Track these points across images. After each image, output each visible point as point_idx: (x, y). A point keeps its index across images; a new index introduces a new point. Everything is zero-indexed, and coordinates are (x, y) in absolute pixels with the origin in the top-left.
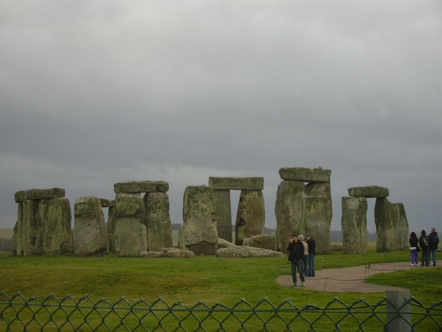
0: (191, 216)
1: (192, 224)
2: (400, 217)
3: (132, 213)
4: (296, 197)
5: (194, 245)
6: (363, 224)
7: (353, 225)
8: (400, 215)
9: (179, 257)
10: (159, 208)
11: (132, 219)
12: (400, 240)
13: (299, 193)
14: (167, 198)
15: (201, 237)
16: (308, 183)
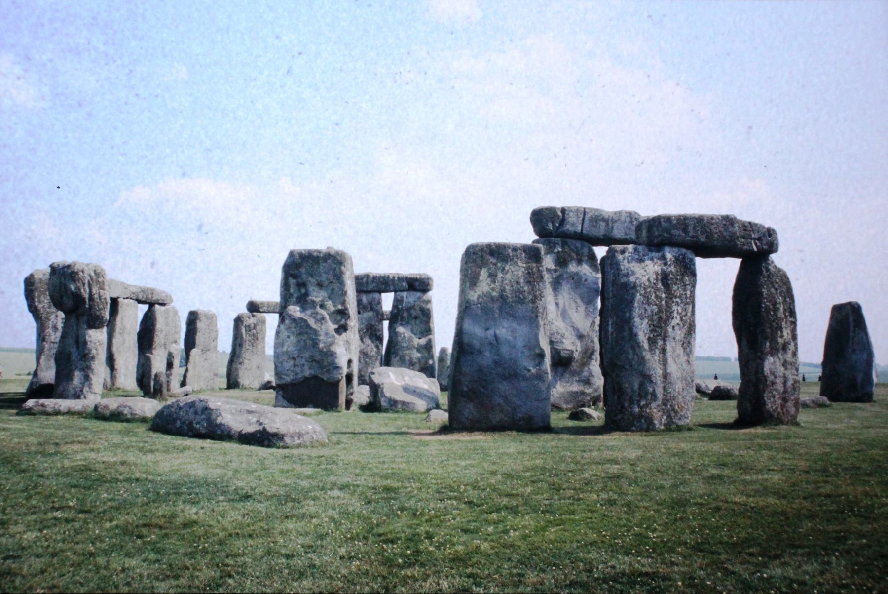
0: (287, 317)
6: (676, 332)
7: (633, 336)
10: (416, 318)
15: (306, 368)
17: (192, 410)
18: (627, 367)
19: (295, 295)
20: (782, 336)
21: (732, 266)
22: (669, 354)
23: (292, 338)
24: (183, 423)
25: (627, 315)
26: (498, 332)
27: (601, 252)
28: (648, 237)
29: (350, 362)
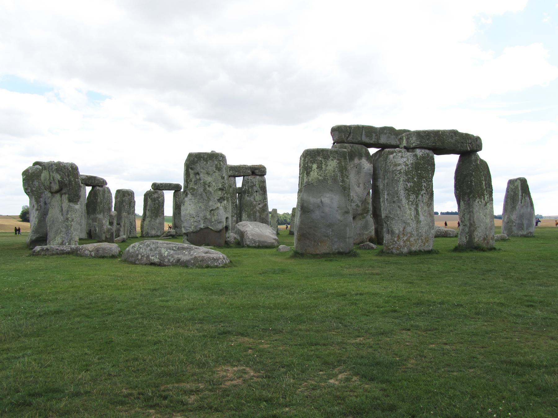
0: (188, 192)
1: (190, 205)
2: (522, 195)
3: (56, 187)
4: (352, 166)
5: (193, 232)
7: (400, 201)
8: (522, 193)
9: (86, 256)
10: (257, 192)
11: (63, 196)
12: (522, 224)
13: (356, 161)
14: (264, 182)
15: (202, 222)
16: (379, 149)
17: (149, 248)
18: (396, 218)
19: (193, 180)
20: (484, 200)
21: (453, 159)
22: (420, 210)
23: (192, 205)
24: (142, 256)
25: (396, 189)
26: (323, 200)
27: (372, 151)
28: (407, 142)
29: (227, 218)
